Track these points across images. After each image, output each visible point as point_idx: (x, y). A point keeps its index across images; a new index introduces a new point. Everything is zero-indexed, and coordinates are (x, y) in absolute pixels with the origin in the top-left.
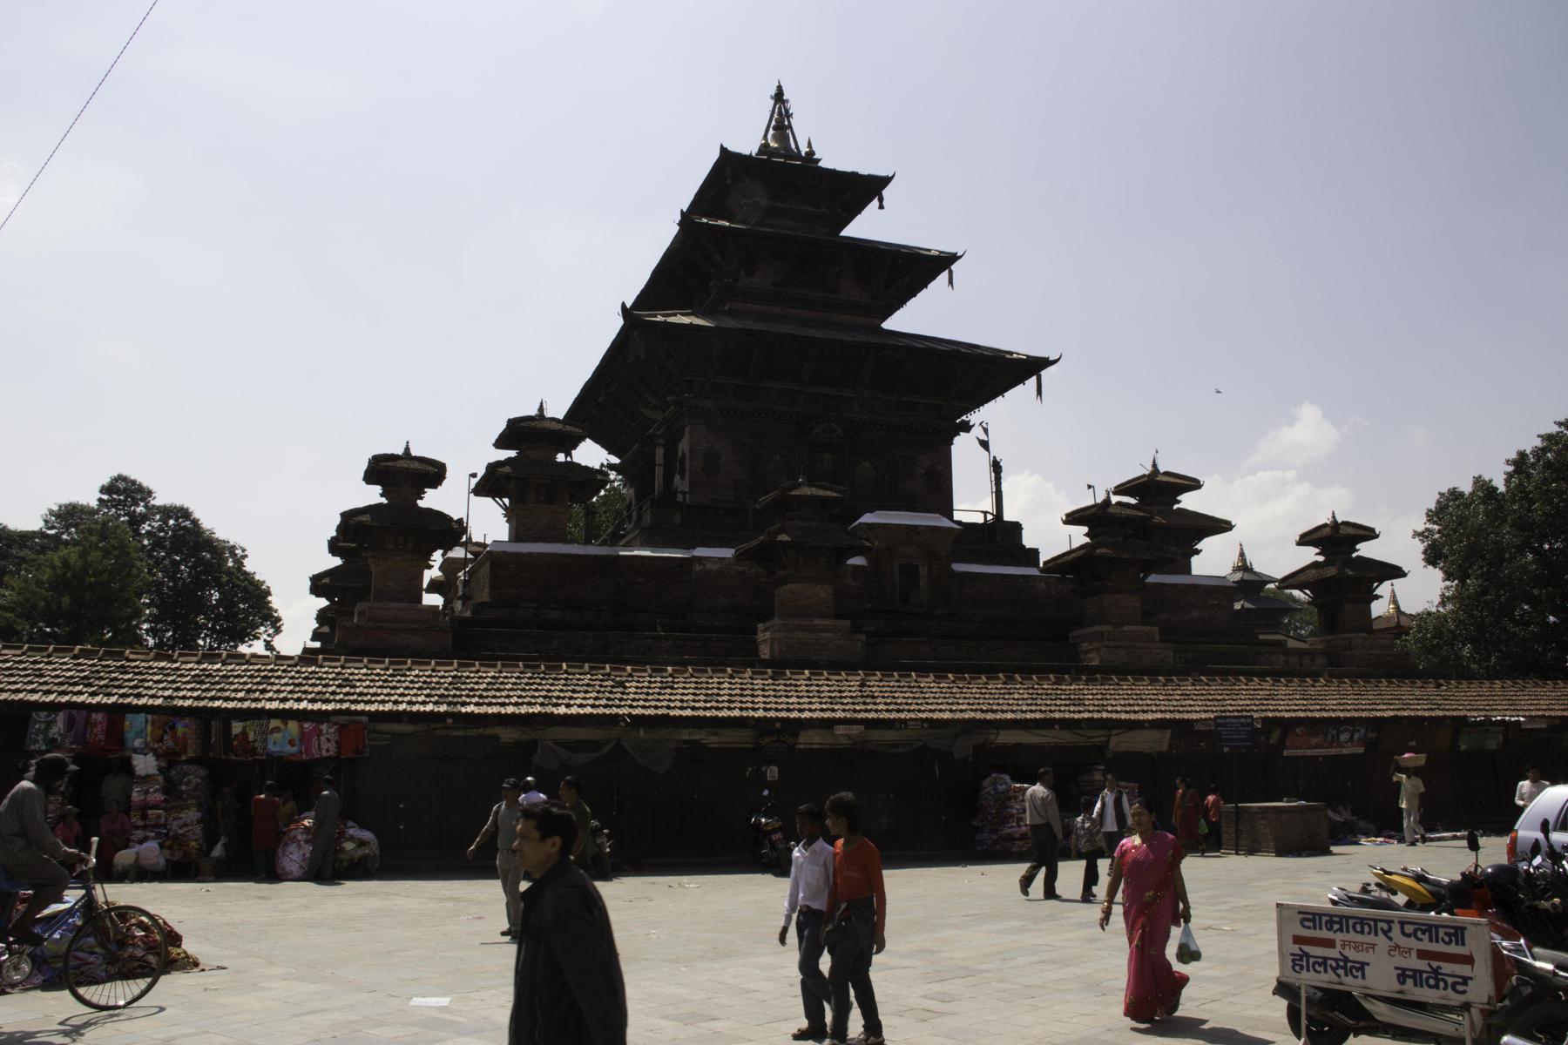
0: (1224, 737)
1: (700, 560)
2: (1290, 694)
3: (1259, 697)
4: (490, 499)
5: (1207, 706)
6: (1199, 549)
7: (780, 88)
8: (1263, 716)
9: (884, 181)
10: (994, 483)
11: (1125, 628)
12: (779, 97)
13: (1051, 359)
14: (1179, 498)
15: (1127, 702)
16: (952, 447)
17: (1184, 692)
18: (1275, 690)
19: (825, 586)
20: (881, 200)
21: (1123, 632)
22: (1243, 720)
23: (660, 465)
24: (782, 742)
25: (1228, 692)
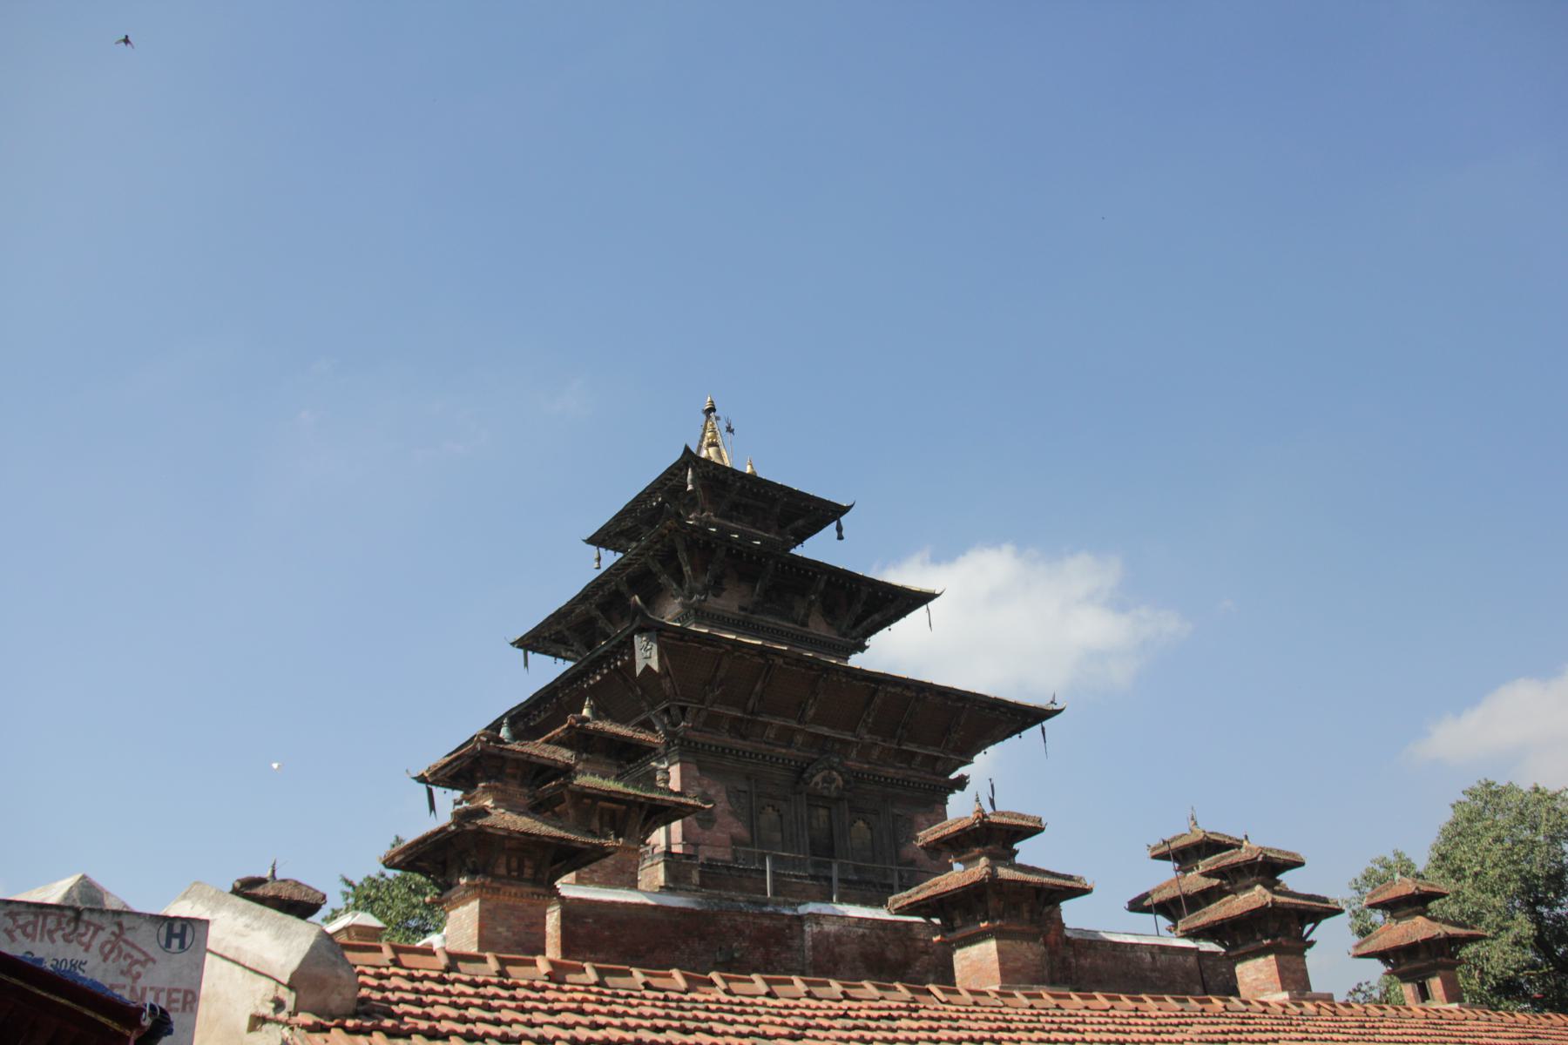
1: (816, 918)
9: (844, 510)
16: (947, 806)
19: (1031, 944)
20: (839, 529)
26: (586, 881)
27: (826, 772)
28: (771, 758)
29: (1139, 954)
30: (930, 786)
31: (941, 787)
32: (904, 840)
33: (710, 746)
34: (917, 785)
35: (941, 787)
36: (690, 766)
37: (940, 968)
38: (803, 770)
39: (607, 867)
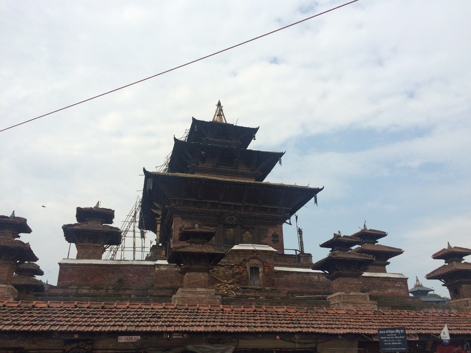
0: (386, 344)
2: (435, 320)
3: (416, 321)
4: (74, 243)
5: (381, 326)
6: (388, 262)
7: (219, 102)
8: (418, 332)
9: (255, 130)
10: (299, 238)
11: (351, 294)
12: (219, 104)
13: (320, 188)
14: (377, 240)
15: (328, 322)
17: (367, 318)
18: (426, 318)
19: (204, 273)
21: (351, 295)
22: (397, 331)
23: (158, 231)
24: (81, 348)
25: (396, 319)
26: (81, 258)
27: (229, 216)
28: (208, 213)
29: (311, 276)
30: (274, 218)
31: (279, 219)
32: (263, 237)
33: (185, 211)
34: (269, 218)
35: (279, 219)
36: (178, 218)
37: (211, 281)
38: (222, 216)
39: (89, 253)
